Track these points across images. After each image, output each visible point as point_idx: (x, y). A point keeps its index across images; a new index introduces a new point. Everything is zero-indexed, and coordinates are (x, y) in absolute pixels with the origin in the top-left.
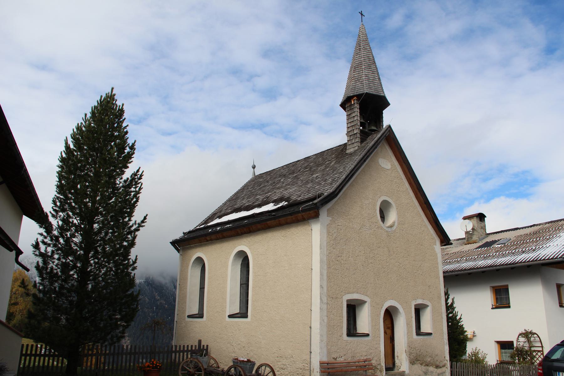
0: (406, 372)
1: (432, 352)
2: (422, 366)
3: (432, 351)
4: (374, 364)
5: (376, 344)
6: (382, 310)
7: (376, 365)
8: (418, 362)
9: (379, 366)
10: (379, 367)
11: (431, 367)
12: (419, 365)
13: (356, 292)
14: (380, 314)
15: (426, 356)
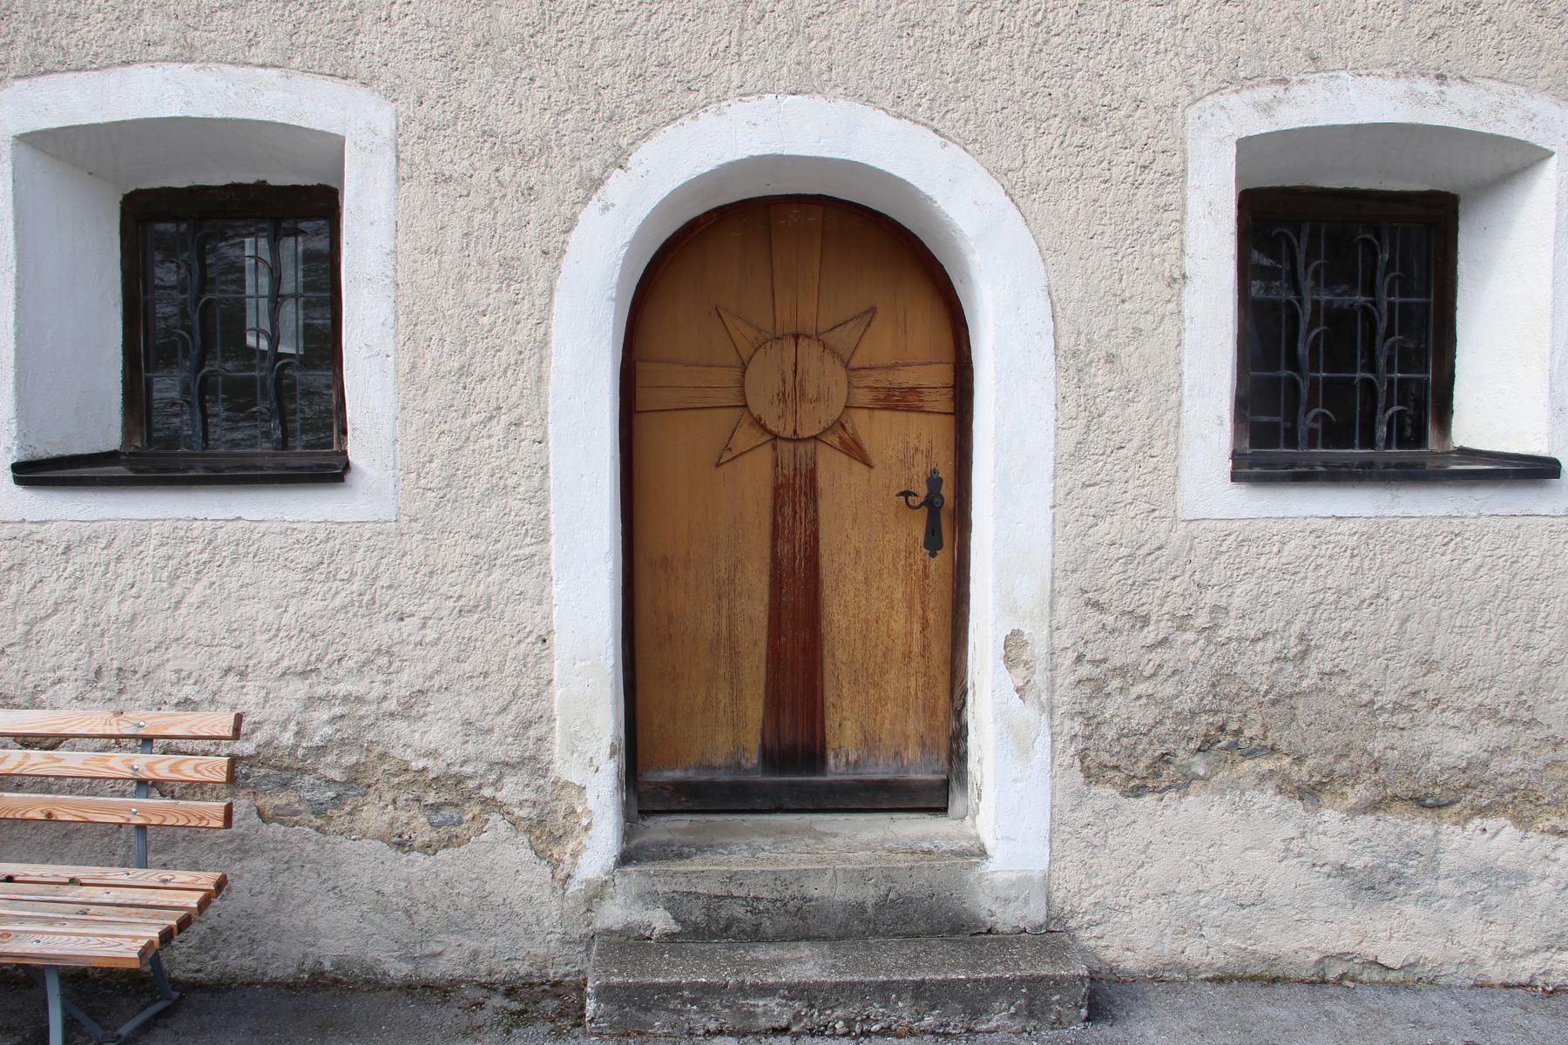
0: (989, 866)
1: (1546, 663)
2: (1317, 805)
3: (1535, 656)
4: (432, 754)
5: (482, 563)
6: (590, 216)
7: (468, 769)
8: (1247, 765)
9: (523, 776)
10: (511, 790)
11: (1491, 823)
12: (1268, 799)
13: (163, 51)
14: (553, 254)
15: (1398, 707)
